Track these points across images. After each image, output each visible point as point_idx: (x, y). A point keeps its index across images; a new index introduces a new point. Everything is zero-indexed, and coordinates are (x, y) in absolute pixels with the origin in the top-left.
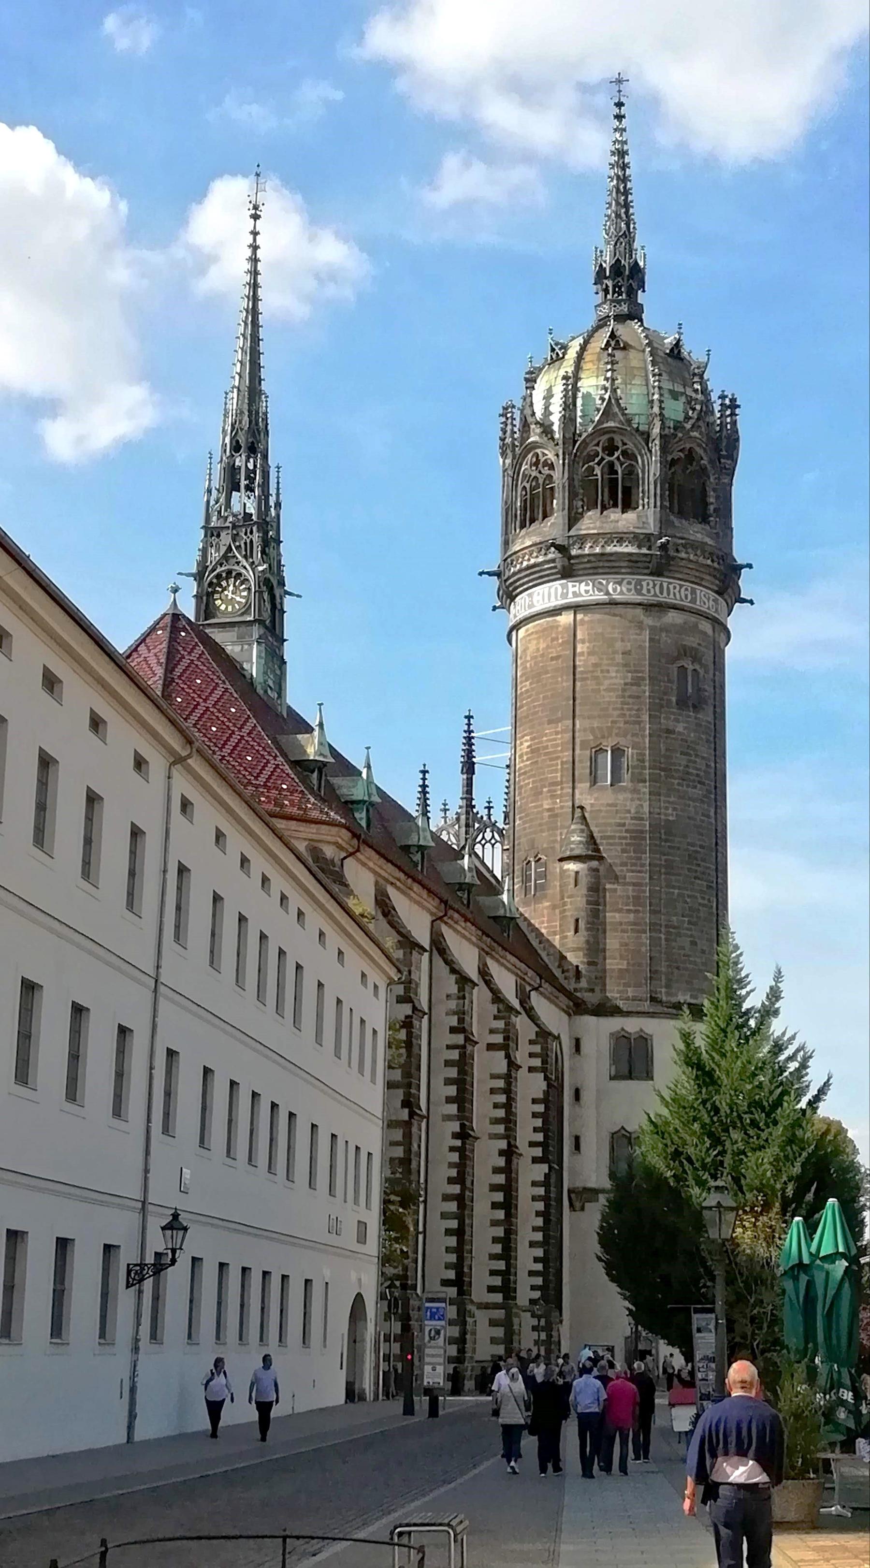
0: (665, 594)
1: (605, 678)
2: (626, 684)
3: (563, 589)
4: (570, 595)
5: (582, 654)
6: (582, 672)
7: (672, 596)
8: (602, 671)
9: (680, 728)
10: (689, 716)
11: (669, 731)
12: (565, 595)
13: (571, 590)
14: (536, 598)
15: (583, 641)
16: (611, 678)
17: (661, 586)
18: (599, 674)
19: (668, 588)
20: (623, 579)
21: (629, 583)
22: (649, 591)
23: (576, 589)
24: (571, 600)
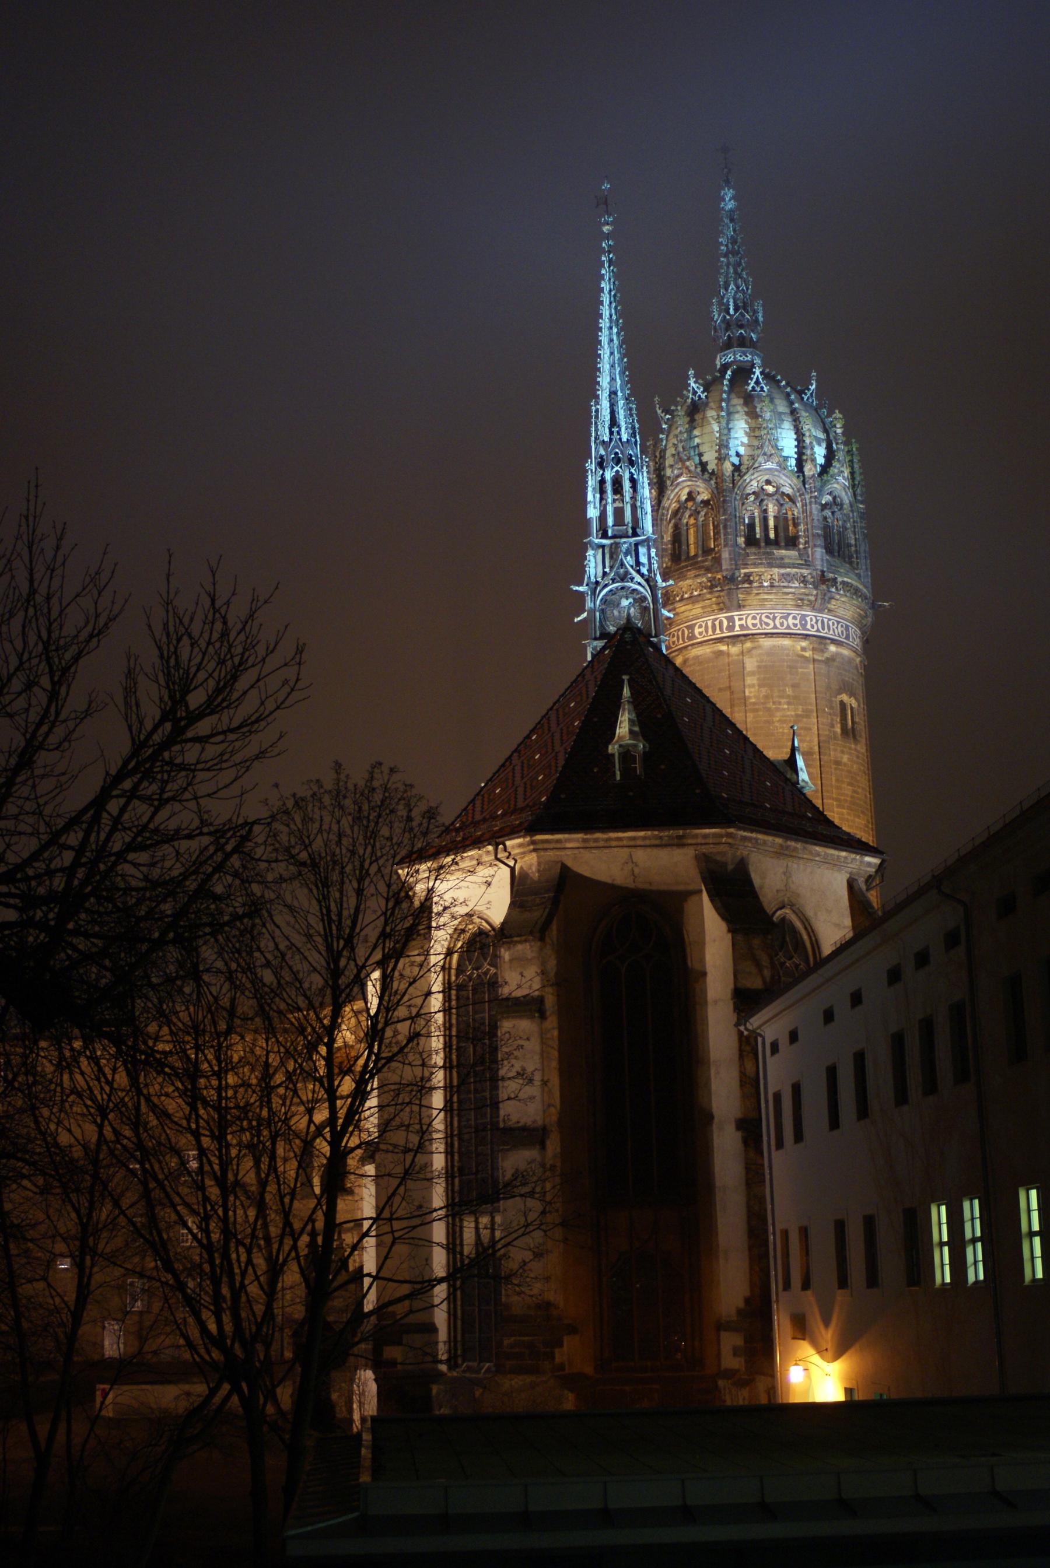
0: (826, 630)
1: (778, 710)
2: (797, 716)
3: (728, 623)
4: (737, 628)
5: (753, 686)
6: (754, 704)
7: (831, 632)
8: (774, 703)
9: (845, 758)
10: (850, 748)
11: (838, 763)
12: (731, 628)
13: (737, 623)
14: (697, 631)
15: (752, 674)
16: (784, 709)
17: (823, 622)
18: (771, 705)
19: (828, 624)
20: (790, 614)
21: (794, 618)
22: (812, 626)
23: (743, 622)
24: (737, 631)
